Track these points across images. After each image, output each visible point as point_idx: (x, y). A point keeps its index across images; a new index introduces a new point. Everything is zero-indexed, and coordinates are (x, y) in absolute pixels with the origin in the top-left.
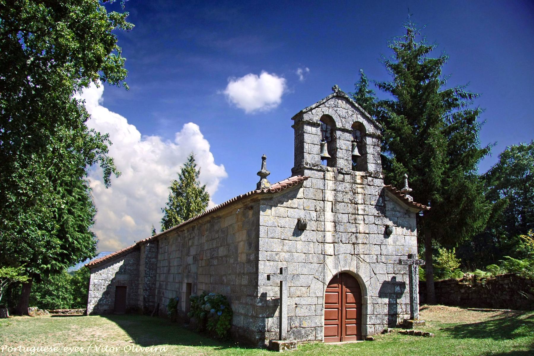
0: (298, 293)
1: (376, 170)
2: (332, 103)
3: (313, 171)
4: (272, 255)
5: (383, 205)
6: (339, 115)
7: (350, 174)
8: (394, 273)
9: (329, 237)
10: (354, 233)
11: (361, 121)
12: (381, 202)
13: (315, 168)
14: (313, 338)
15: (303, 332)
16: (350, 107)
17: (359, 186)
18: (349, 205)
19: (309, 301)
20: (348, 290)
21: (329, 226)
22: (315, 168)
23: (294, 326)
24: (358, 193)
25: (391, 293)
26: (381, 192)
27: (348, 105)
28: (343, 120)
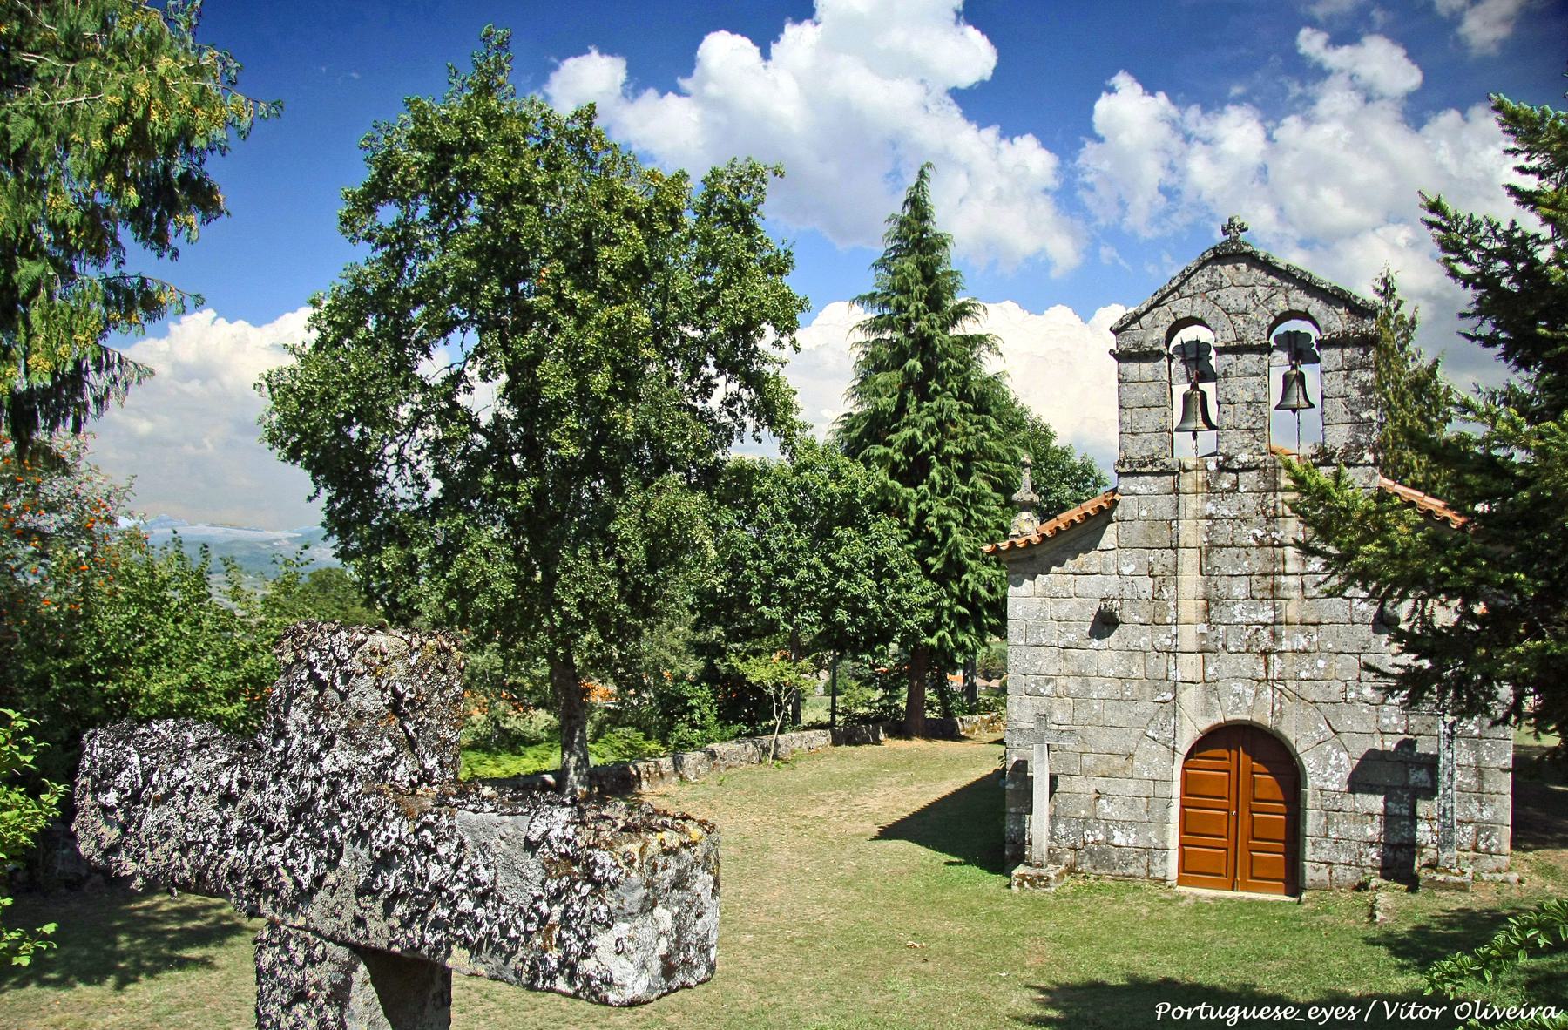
0: (1103, 768)
1: (1356, 440)
2: (1203, 281)
4: (1037, 682)
6: (1226, 311)
7: (1257, 467)
8: (1406, 732)
9: (1189, 637)
10: (1265, 625)
11: (1301, 308)
13: (1149, 468)
14: (1142, 872)
15: (1115, 855)
16: (1264, 275)
18: (1254, 552)
19: (1132, 787)
20: (1261, 768)
21: (1190, 609)
22: (1149, 468)
23: (1091, 839)
25: (1394, 788)
27: (1256, 272)
28: (1239, 321)
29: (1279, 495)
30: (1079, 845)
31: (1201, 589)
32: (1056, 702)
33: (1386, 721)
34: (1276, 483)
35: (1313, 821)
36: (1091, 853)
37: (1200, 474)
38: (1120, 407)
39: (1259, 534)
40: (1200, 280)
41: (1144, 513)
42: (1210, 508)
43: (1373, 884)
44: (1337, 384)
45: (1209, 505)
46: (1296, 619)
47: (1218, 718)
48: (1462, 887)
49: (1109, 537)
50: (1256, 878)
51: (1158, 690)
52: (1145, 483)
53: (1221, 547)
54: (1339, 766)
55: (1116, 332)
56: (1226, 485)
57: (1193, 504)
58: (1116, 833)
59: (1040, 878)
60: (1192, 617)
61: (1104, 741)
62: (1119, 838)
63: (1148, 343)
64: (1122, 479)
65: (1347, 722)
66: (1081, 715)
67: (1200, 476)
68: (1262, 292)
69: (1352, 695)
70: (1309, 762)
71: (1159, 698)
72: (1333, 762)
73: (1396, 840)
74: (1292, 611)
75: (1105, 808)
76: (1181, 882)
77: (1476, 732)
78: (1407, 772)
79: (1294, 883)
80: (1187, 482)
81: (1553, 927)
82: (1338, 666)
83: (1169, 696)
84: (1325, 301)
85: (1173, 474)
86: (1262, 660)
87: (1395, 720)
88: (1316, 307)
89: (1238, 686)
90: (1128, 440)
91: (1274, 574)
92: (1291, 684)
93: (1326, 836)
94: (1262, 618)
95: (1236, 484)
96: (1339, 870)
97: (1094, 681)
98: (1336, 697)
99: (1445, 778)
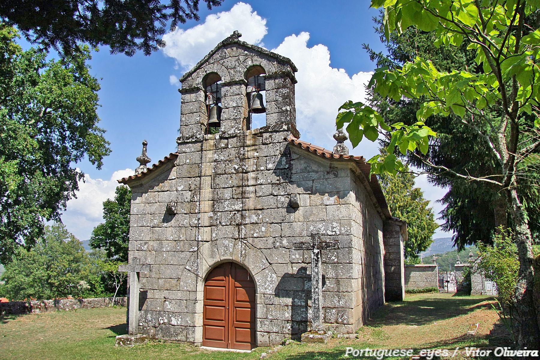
0: (167, 286)
3: (188, 145)
4: (141, 244)
5: (287, 166)
6: (227, 68)
7: (236, 136)
8: (303, 262)
9: (205, 219)
10: (238, 211)
11: (258, 63)
12: (284, 163)
14: (184, 338)
15: (172, 330)
16: (243, 51)
17: (249, 149)
18: (234, 176)
19: (179, 295)
20: (237, 284)
21: (206, 206)
23: (162, 322)
24: (248, 158)
25: (297, 291)
26: (286, 149)
27: (240, 50)
28: (232, 71)
29: (246, 148)
30: (157, 325)
31: (211, 196)
32: (148, 253)
33: (294, 257)
34: (245, 142)
35: (260, 311)
36: (161, 329)
37: (212, 141)
38: (181, 114)
39: (237, 167)
40: (217, 56)
41: (188, 161)
42: (216, 157)
43: (287, 342)
44: (272, 94)
45: (216, 155)
46: (252, 207)
47: (217, 259)
48: (321, 341)
49: (173, 174)
50: (239, 343)
51: (191, 246)
52: (189, 147)
53: (220, 174)
54: (272, 281)
55: (182, 81)
56: (223, 145)
57: (210, 155)
58: (172, 318)
59: (128, 340)
60: (207, 209)
61: (168, 272)
62: (174, 322)
63: (194, 85)
64: (180, 146)
65: (275, 259)
66: (159, 259)
67: (212, 142)
68: (242, 58)
69: (278, 244)
70: (258, 279)
71: (192, 250)
72: (269, 279)
73: (299, 319)
74: (251, 203)
75: (169, 306)
76: (203, 344)
77: (336, 260)
78: (304, 283)
79: (254, 343)
80: (206, 145)
81: (1, 297)
82: (271, 230)
83: (196, 249)
84: (268, 60)
85: (201, 142)
86: (237, 228)
87: (297, 256)
88: (264, 63)
89: (226, 242)
90: (183, 129)
91: (243, 186)
92: (250, 240)
93: (267, 318)
94: (237, 208)
95: (227, 145)
96: (273, 336)
97: (165, 243)
98: (270, 245)
99: (315, 283)
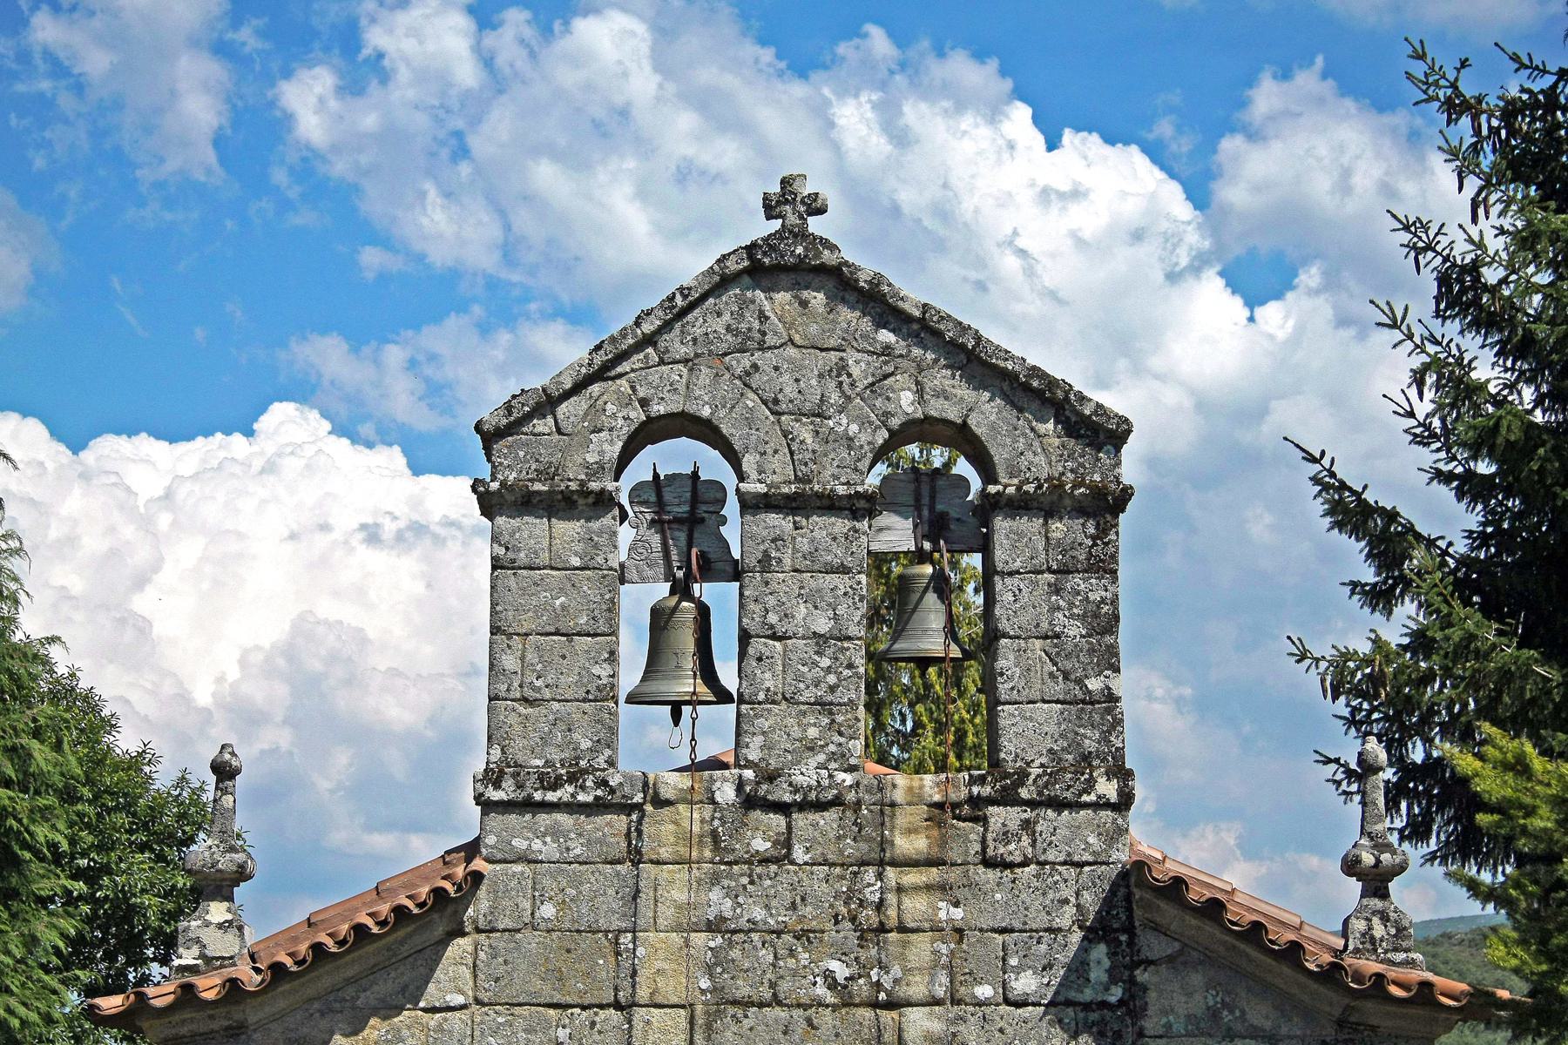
1: (1075, 745)
2: (719, 325)
3: (544, 819)
5: (1116, 993)
6: (772, 404)
7: (837, 802)
11: (953, 414)
12: (1098, 974)
13: (565, 793)
16: (866, 324)
17: (913, 877)
18: (826, 1018)
22: (565, 793)
24: (902, 929)
26: (1108, 903)
29: (890, 872)
34: (884, 844)
38: (495, 630)
39: (841, 971)
40: (710, 323)
41: (548, 911)
42: (718, 902)
45: (715, 895)
52: (555, 832)
53: (746, 1004)
56: (761, 845)
63: (573, 475)
64: (496, 820)
67: (694, 818)
80: (662, 832)
85: (627, 808)
88: (988, 415)
90: (512, 718)
95: (786, 841)
